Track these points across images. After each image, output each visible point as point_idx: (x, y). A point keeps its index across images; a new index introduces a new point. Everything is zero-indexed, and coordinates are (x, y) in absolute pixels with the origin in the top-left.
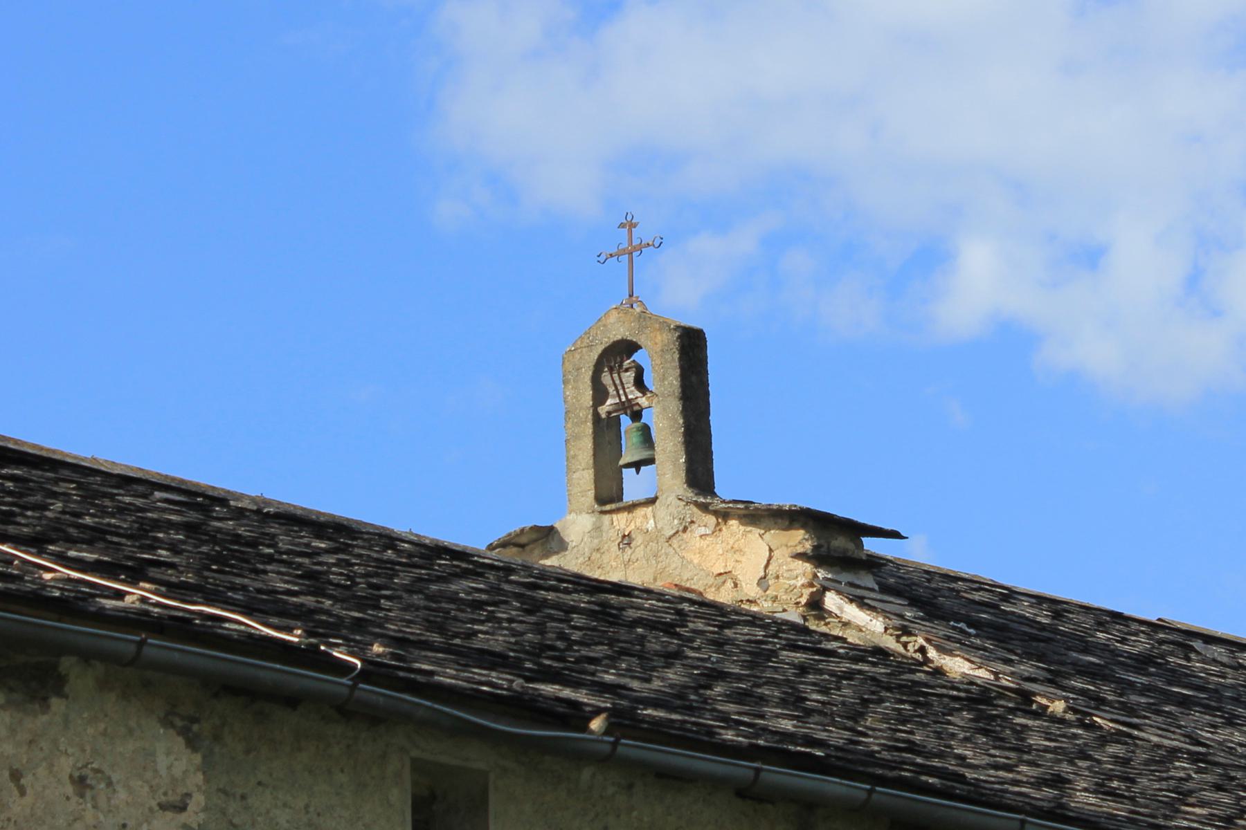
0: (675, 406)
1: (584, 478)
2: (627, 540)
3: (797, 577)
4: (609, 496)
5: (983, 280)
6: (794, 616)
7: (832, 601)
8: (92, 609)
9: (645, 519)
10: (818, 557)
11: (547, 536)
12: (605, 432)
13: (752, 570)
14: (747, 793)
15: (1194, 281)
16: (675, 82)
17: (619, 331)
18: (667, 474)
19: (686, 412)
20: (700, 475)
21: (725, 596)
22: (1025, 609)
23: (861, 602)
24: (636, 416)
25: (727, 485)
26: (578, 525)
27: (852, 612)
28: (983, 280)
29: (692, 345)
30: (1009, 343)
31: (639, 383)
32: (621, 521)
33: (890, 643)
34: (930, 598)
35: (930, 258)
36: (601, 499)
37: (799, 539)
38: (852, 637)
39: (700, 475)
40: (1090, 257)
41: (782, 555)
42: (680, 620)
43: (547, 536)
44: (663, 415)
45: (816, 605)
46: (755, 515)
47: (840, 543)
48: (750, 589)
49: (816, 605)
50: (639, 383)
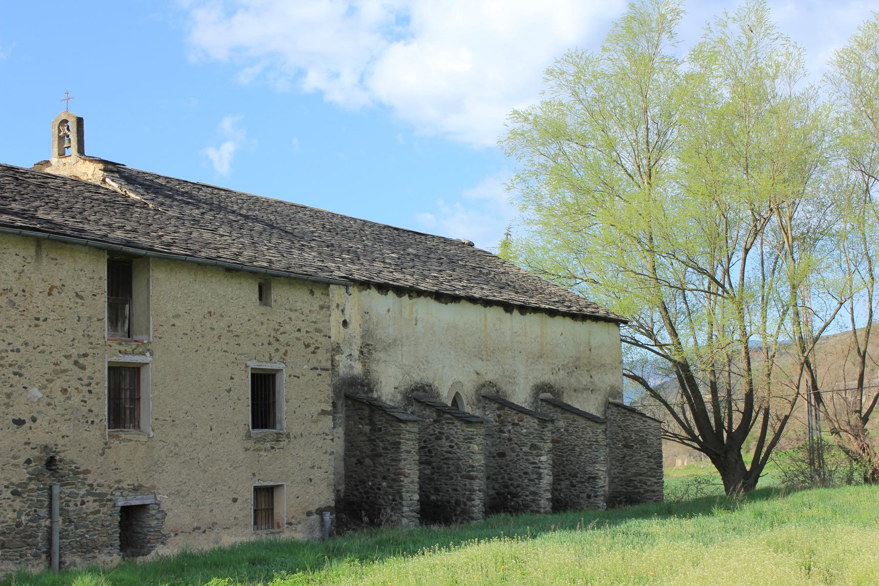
0: (75, 135)
1: (56, 150)
2: (65, 164)
3: (100, 174)
4: (62, 154)
5: (313, 80)
6: (99, 183)
7: (107, 180)
8: (227, 123)
9: (68, 160)
10: (105, 170)
11: (47, 163)
12: (61, 139)
13: (91, 173)
14: (19, 234)
15: (361, 81)
16: (247, 30)
17: (64, 117)
18: (73, 150)
19: (78, 136)
20: (81, 150)
21: (84, 178)
22: (160, 181)
23: (113, 180)
24: (68, 136)
25: (87, 152)
26: (54, 160)
27: (113, 184)
28: (313, 80)
29: (80, 122)
30: (319, 94)
31: (68, 129)
32: (63, 160)
33: (119, 190)
34: (130, 178)
35: (301, 73)
36: (59, 155)
37: (101, 166)
38: (110, 188)
39: (81, 150)
40: (336, 75)
41: (97, 169)
42: (76, 182)
43: (47, 163)
44: (73, 136)
45: (104, 181)
46: (93, 160)
47: (110, 167)
48: (90, 177)
49: (104, 181)
50: (68, 129)
